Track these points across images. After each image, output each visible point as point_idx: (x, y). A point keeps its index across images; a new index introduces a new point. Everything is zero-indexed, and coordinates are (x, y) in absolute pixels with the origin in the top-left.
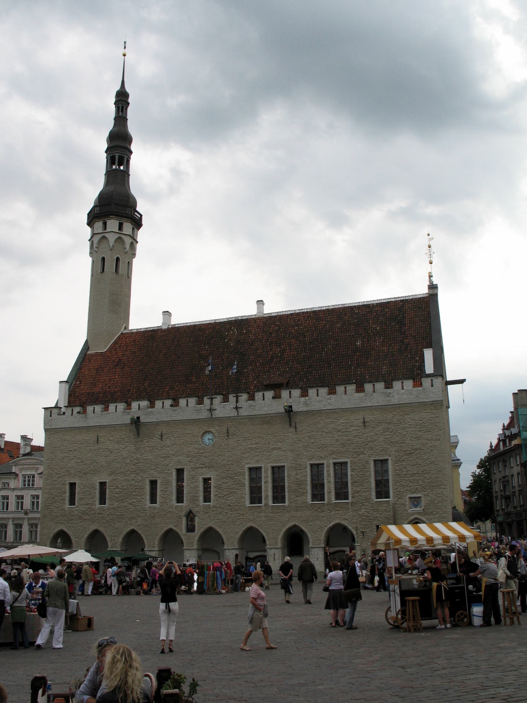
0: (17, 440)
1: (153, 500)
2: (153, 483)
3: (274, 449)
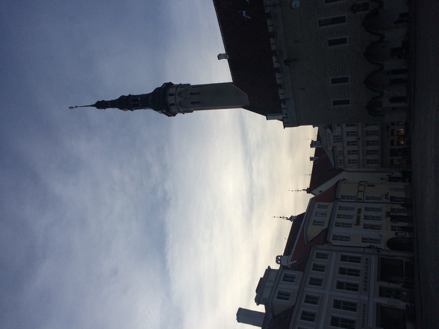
0: (314, 149)
1: (343, 41)
2: (331, 43)
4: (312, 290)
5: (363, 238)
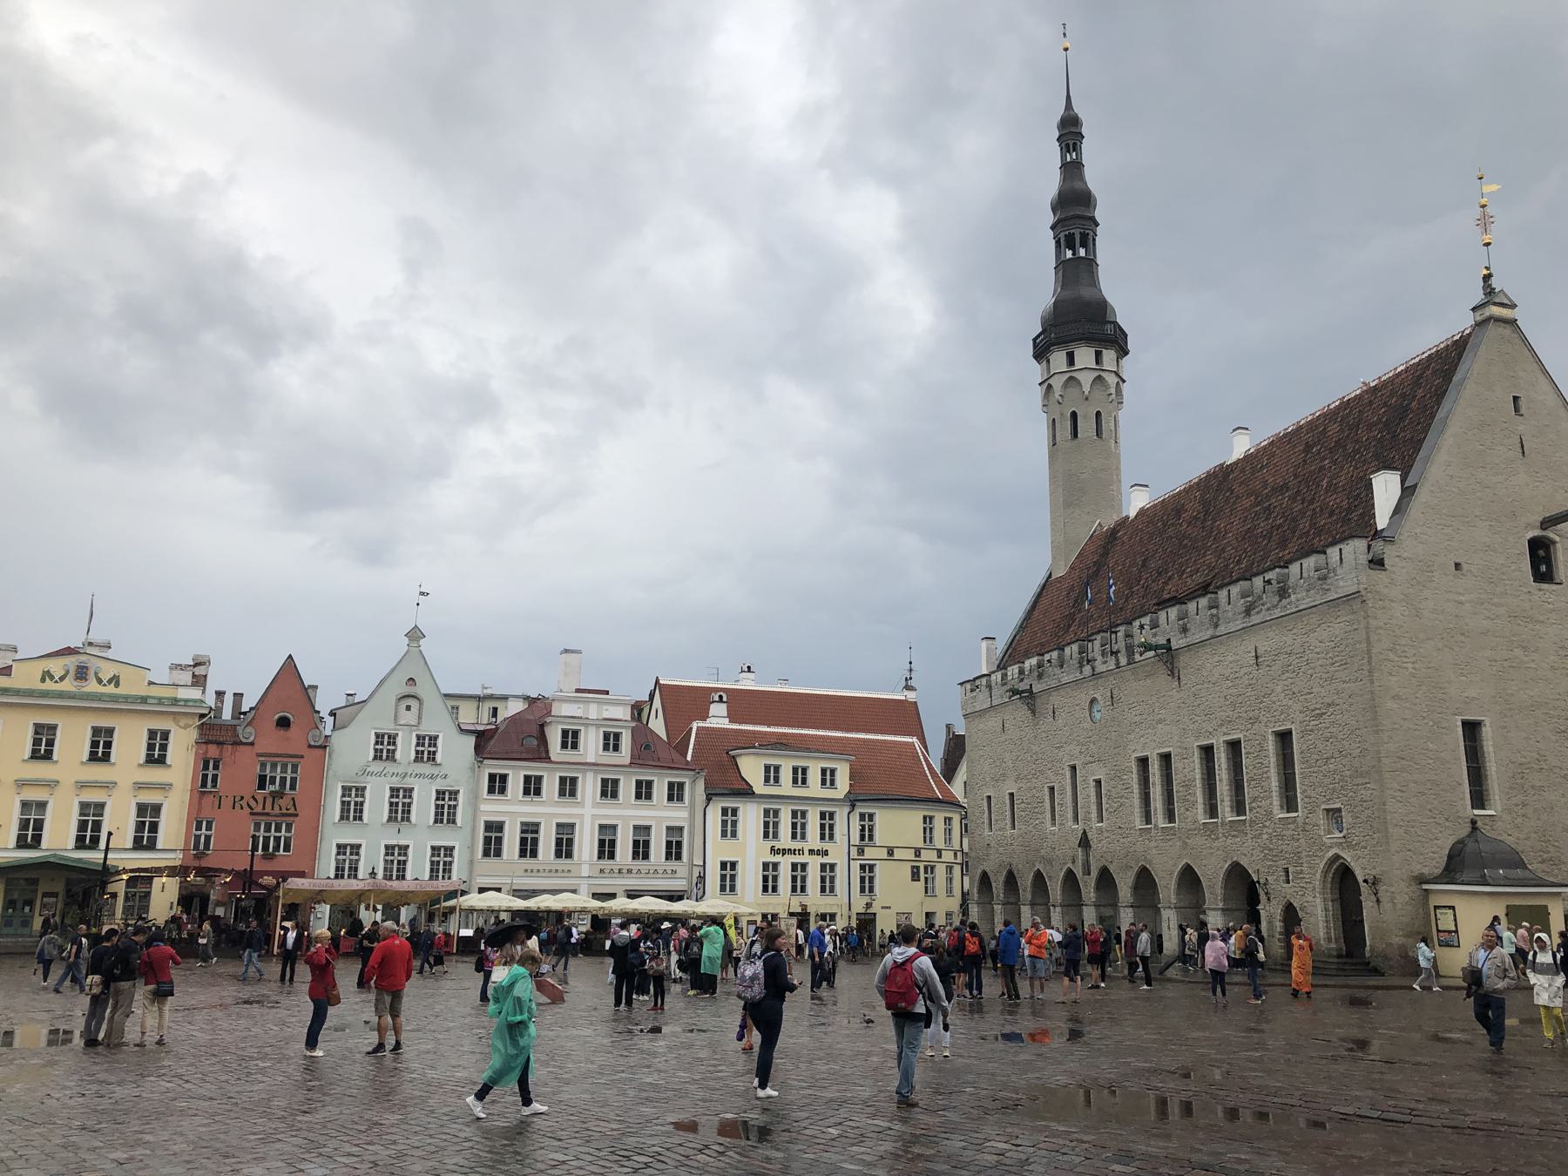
3: (1160, 722)
4: (589, 786)
5: (733, 865)
